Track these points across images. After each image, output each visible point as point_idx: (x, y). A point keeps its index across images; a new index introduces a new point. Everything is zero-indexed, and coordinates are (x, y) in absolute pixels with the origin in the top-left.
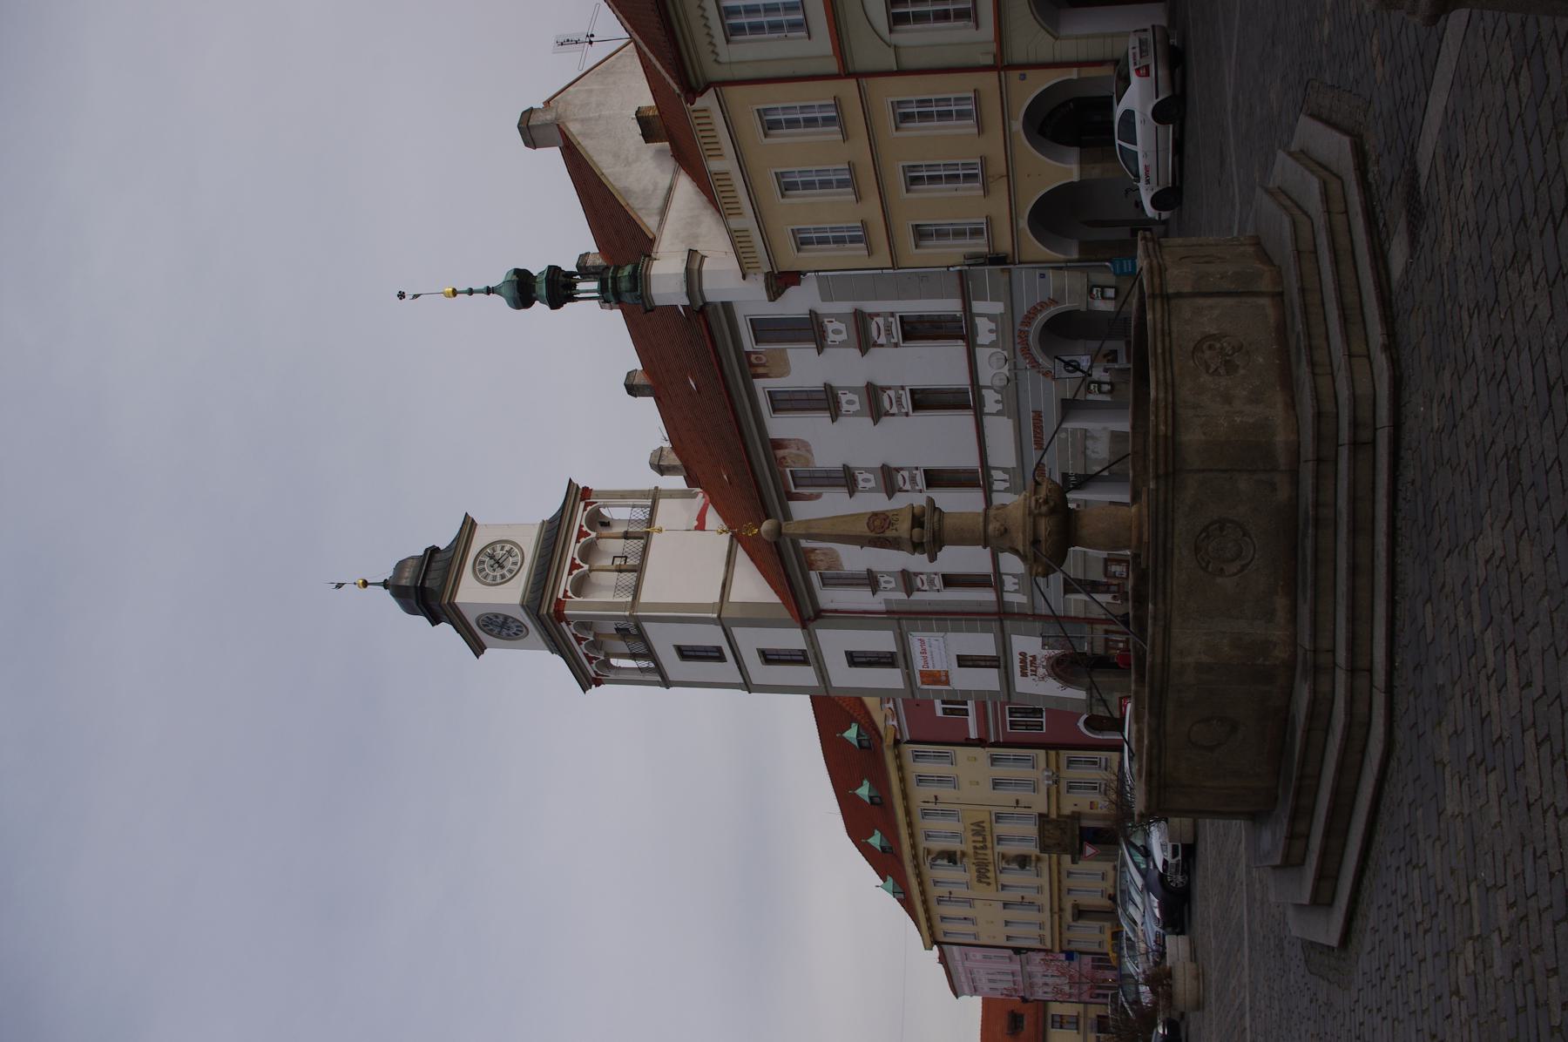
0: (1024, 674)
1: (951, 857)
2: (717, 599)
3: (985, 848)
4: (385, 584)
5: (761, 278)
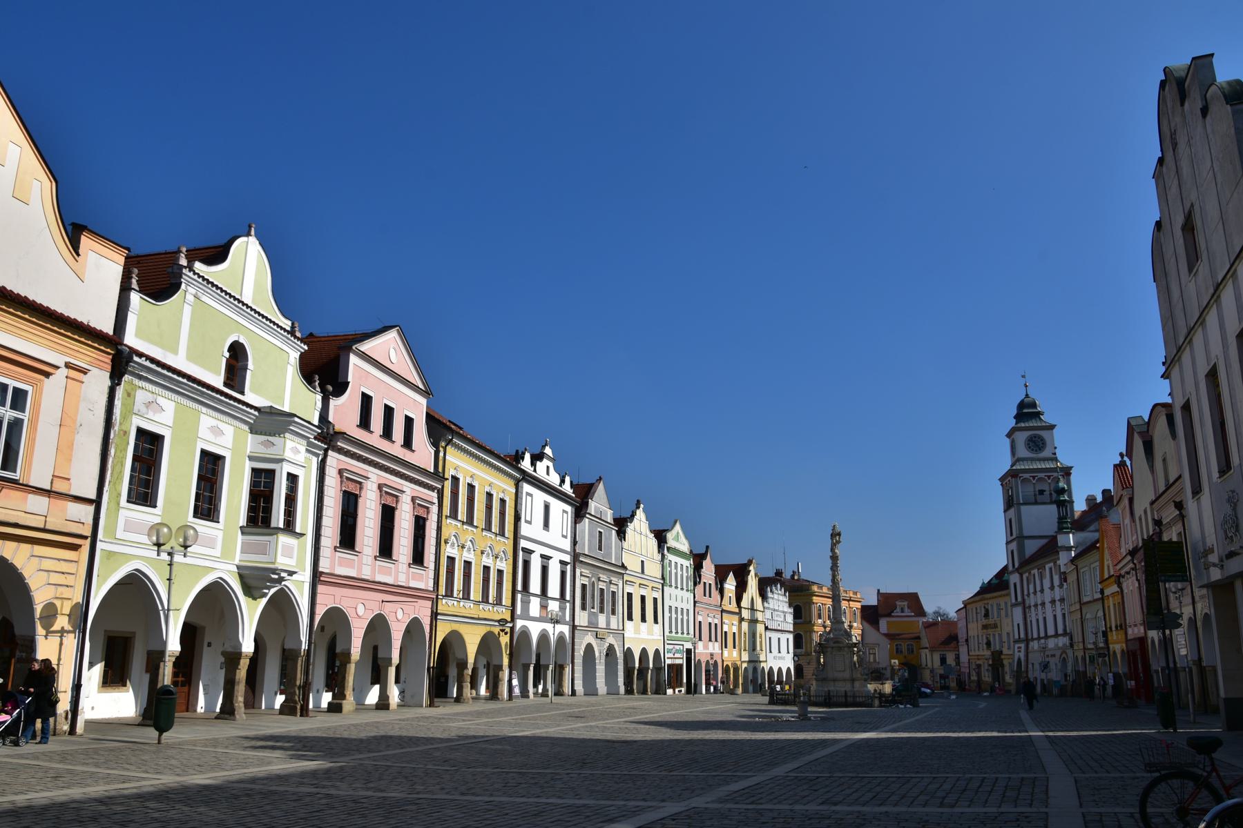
0: (1019, 648)
1: (986, 615)
2: (1025, 534)
3: (992, 628)
4: (1027, 396)
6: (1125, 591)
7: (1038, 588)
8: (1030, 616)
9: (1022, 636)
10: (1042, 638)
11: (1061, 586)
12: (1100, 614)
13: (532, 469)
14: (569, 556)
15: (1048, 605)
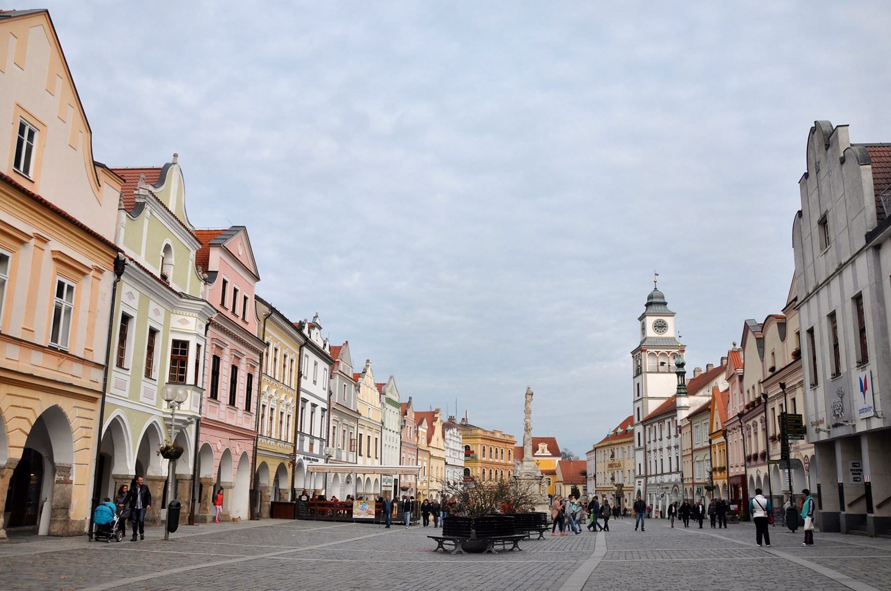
1: (613, 456)
2: (649, 396)
3: (616, 467)
5: (680, 425)
6: (729, 442)
7: (658, 437)
8: (650, 458)
9: (643, 473)
10: (659, 475)
11: (676, 436)
12: (708, 457)
13: (309, 336)
14: (326, 404)
15: (665, 450)
